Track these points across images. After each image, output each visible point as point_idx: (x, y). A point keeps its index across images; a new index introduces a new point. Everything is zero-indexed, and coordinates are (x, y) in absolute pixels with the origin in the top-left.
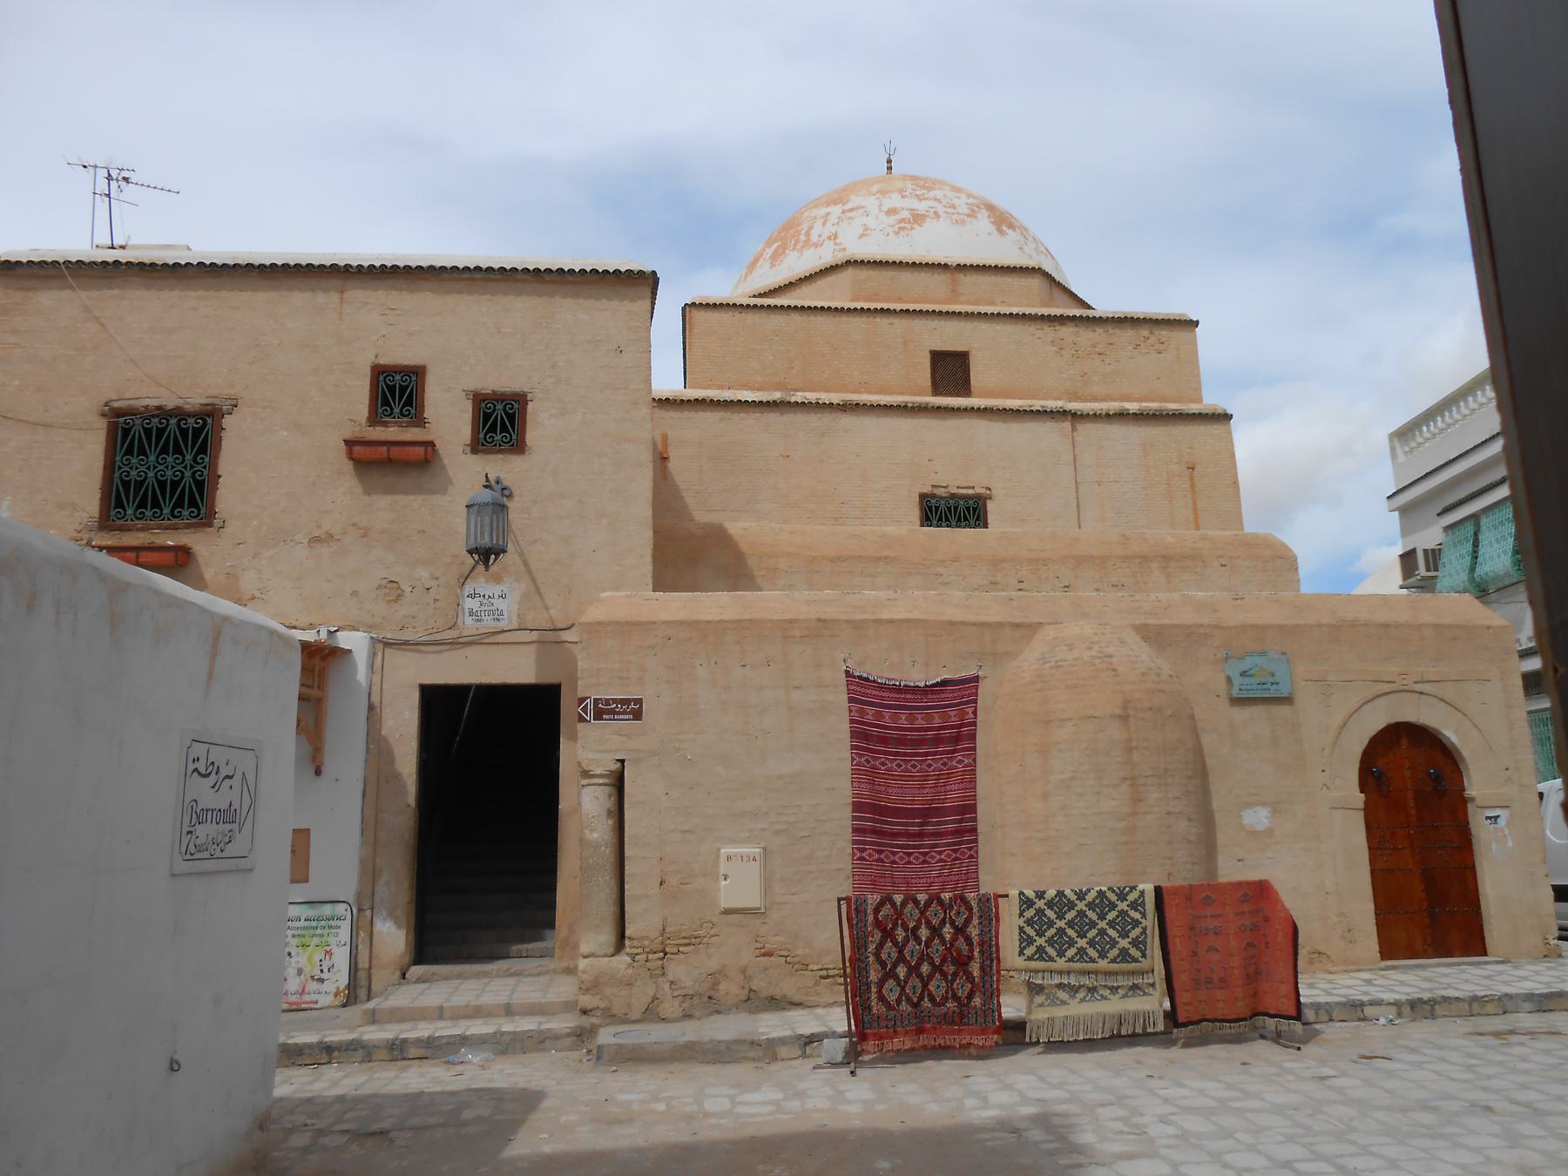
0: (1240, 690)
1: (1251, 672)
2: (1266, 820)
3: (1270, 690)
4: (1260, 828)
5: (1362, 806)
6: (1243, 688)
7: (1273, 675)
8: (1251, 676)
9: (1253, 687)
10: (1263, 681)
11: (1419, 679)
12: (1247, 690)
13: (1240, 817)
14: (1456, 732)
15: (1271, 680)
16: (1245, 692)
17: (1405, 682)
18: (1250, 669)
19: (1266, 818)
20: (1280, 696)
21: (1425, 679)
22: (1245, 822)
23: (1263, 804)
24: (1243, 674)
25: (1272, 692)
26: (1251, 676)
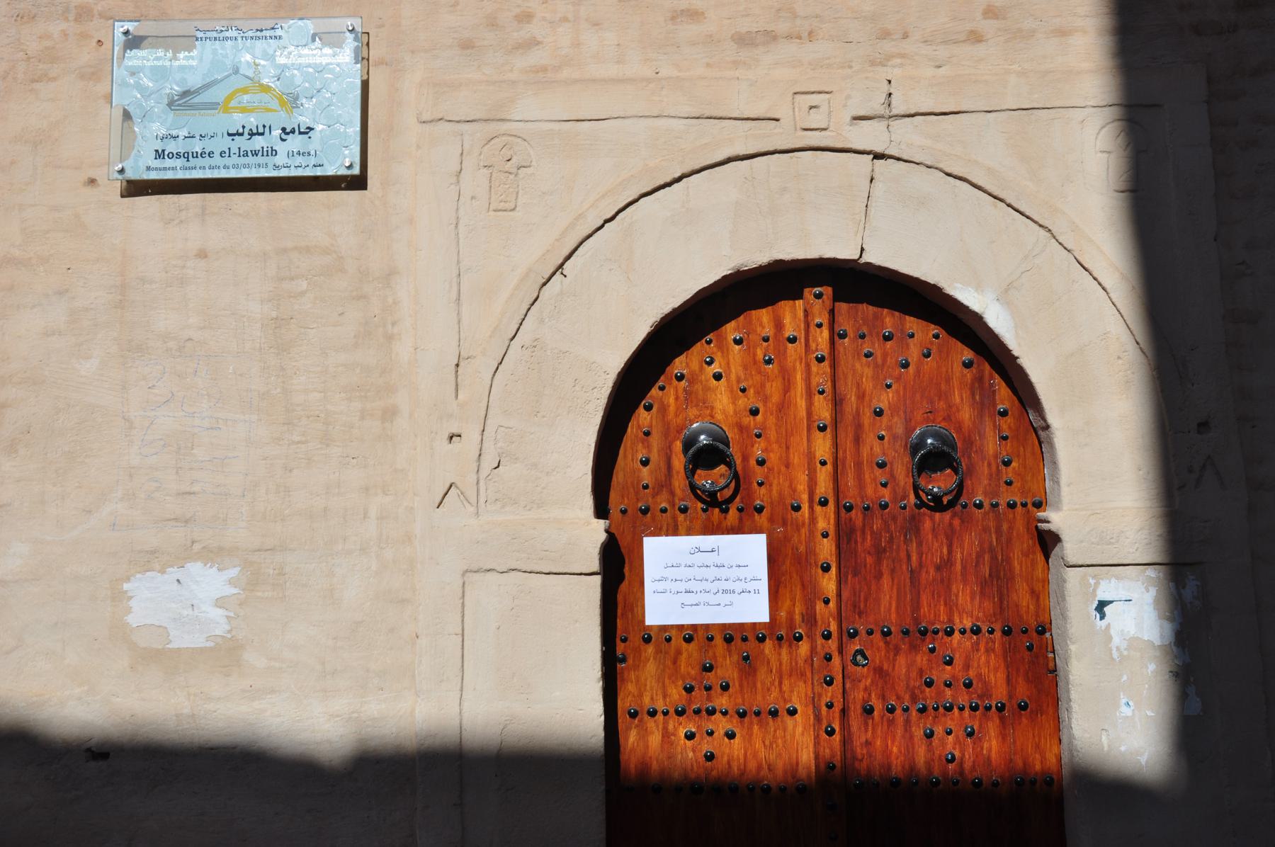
0: (160, 154)
1: (216, 95)
2: (218, 614)
3: (274, 152)
4: (182, 640)
5: (595, 565)
6: (171, 147)
7: (291, 101)
8: (213, 106)
9: (209, 145)
10: (252, 121)
11: (875, 105)
12: (186, 156)
13: (119, 597)
14: (1005, 296)
15: (281, 119)
16: (179, 163)
17: (816, 119)
18: (206, 87)
19: (220, 603)
20: (319, 172)
21: (899, 107)
22: (133, 620)
23: (213, 555)
24: (183, 101)
25: (280, 159)
26: (213, 106)
